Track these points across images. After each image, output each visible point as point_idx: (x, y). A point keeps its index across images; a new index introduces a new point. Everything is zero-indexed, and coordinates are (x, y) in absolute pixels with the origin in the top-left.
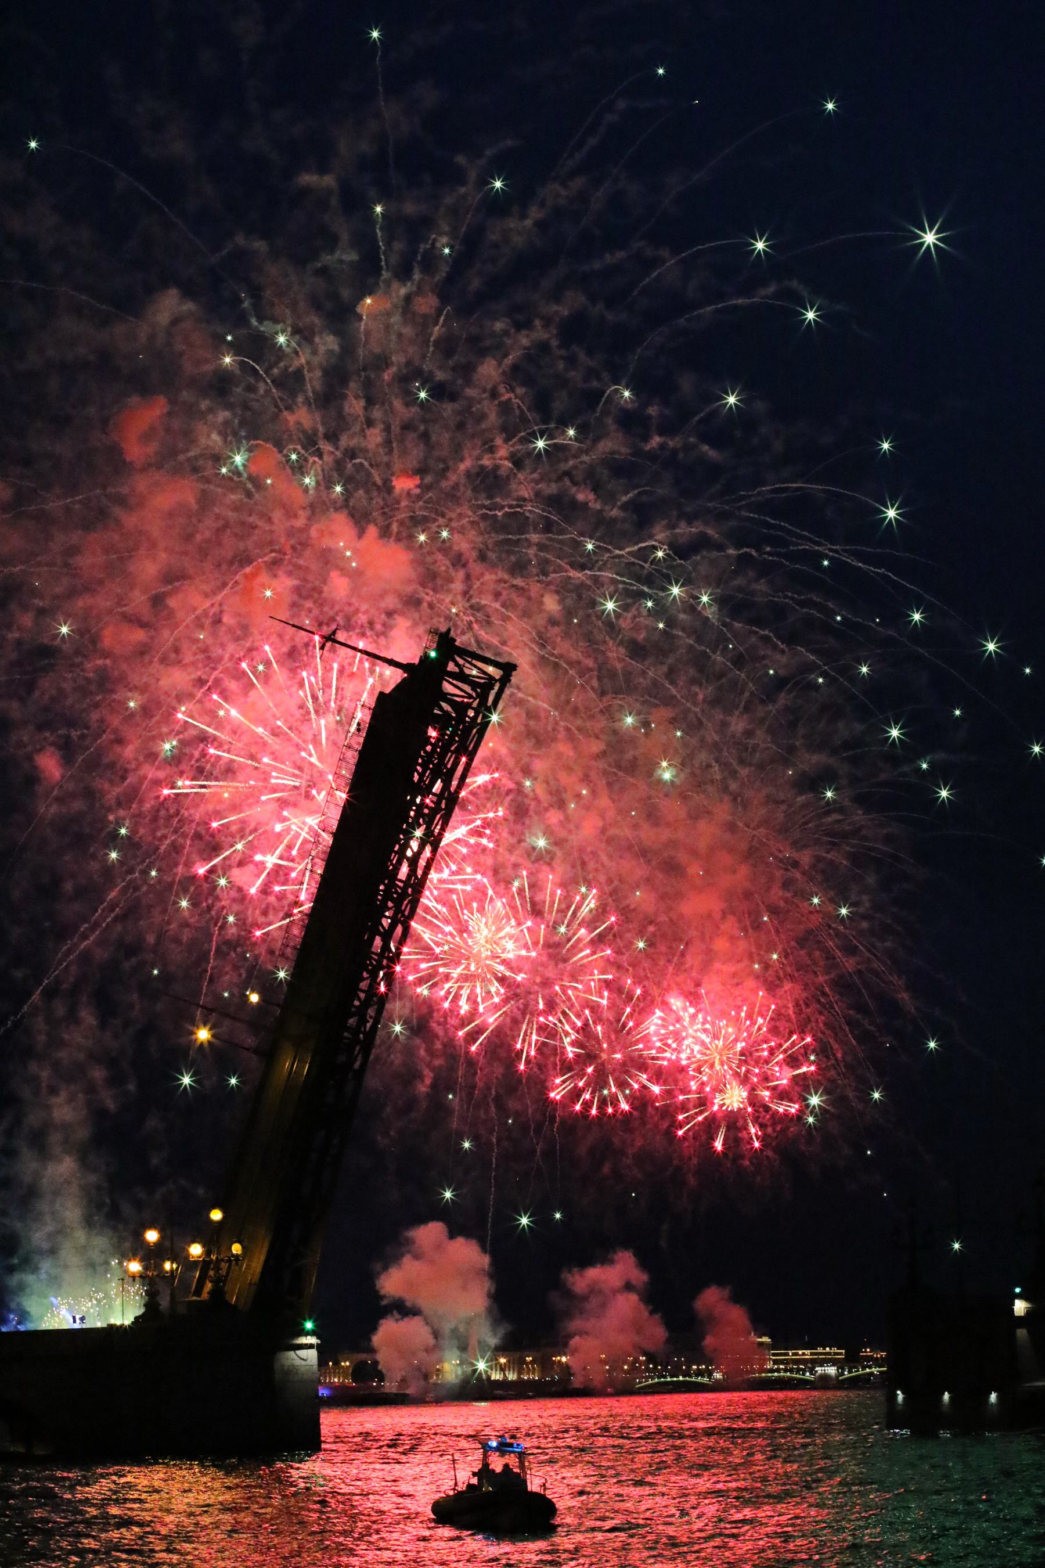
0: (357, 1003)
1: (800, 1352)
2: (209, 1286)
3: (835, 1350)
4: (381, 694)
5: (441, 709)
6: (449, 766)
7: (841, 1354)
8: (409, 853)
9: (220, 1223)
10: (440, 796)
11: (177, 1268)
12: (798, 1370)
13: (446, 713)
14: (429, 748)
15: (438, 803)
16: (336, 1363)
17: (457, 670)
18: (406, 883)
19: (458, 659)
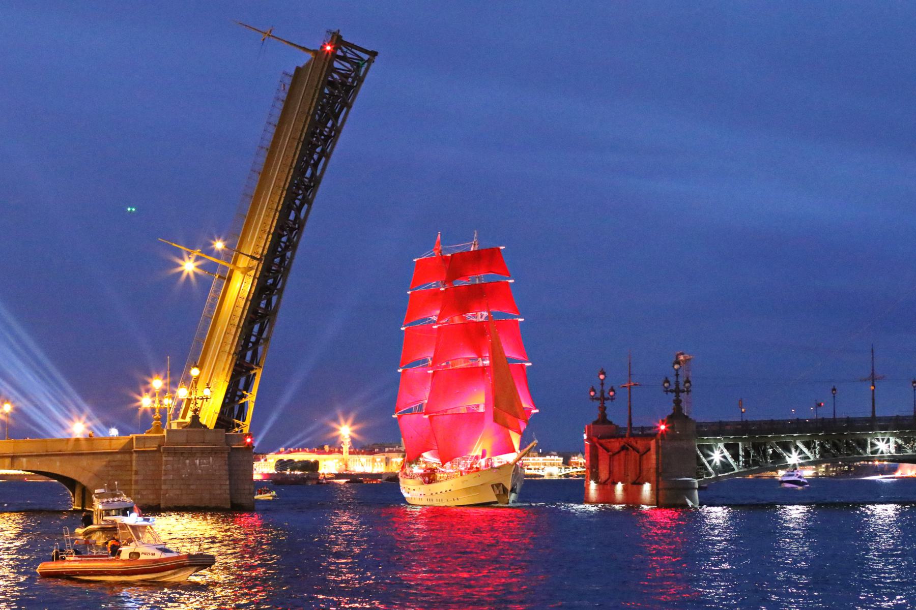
0: (280, 249)
1: (537, 458)
2: (190, 414)
3: (557, 458)
4: (298, 70)
5: (332, 77)
6: (337, 111)
7: (560, 460)
9: (198, 378)
10: (331, 130)
11: (172, 404)
12: (535, 469)
13: (336, 79)
14: (325, 100)
15: (331, 132)
16: (266, 460)
17: (342, 54)
18: (310, 179)
19: (343, 48)
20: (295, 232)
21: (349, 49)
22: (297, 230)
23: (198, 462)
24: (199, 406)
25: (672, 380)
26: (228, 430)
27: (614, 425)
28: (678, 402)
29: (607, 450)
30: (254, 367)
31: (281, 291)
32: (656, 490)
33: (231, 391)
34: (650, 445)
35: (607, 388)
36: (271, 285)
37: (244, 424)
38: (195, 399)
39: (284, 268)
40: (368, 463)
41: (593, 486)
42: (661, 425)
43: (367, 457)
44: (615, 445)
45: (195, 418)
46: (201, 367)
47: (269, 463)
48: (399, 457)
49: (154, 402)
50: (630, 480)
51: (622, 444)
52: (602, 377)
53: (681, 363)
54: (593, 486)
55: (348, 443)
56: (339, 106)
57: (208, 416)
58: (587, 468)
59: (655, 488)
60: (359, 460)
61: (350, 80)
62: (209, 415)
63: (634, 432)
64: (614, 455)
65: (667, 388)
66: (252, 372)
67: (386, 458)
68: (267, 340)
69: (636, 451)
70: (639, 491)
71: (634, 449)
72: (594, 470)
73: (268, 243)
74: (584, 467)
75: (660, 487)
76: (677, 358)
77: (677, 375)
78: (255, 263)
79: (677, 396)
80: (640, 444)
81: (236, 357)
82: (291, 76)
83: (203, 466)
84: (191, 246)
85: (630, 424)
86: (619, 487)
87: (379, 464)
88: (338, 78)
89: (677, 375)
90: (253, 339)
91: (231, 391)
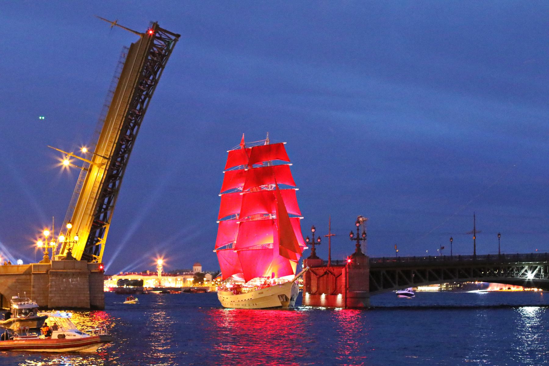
0: (121, 153)
2: (66, 251)
4: (133, 45)
5: (153, 49)
8: (141, 100)
9: (71, 230)
16: (111, 279)
20: (130, 143)
21: (162, 32)
22: (131, 142)
23: (70, 280)
24: (71, 246)
25: (355, 232)
26: (89, 261)
27: (320, 259)
28: (358, 246)
29: (316, 274)
30: (105, 223)
31: (121, 178)
32: (345, 299)
33: (91, 237)
34: (342, 271)
35: (316, 237)
36: (115, 174)
37: (98, 258)
38: (69, 242)
39: (123, 163)
40: (173, 281)
41: (307, 295)
42: (348, 260)
43: (172, 278)
44: (321, 271)
45: (69, 254)
46: (73, 223)
47: (114, 281)
48: (191, 278)
49: (44, 244)
50: (329, 292)
51: (325, 271)
52: (313, 230)
53: (361, 222)
54: (307, 295)
55: (161, 269)
56: (157, 67)
57: (77, 253)
58: (304, 285)
59: (344, 297)
60: (168, 279)
61: (164, 51)
62: (78, 252)
63: (332, 263)
64: (320, 277)
65: (352, 237)
66: (104, 227)
67: (184, 278)
68: (113, 207)
69: (333, 275)
70: (335, 299)
71: (332, 273)
72: (308, 286)
73: (114, 149)
74: (302, 285)
75: (348, 296)
76: (358, 220)
77: (358, 230)
78: (106, 161)
79: (358, 242)
80: (336, 271)
81: (94, 217)
82: (128, 49)
83: (73, 282)
84: (68, 151)
85: (330, 258)
86: (323, 296)
87: (179, 282)
88: (156, 50)
89: (358, 230)
90: (104, 206)
91: (91, 237)
